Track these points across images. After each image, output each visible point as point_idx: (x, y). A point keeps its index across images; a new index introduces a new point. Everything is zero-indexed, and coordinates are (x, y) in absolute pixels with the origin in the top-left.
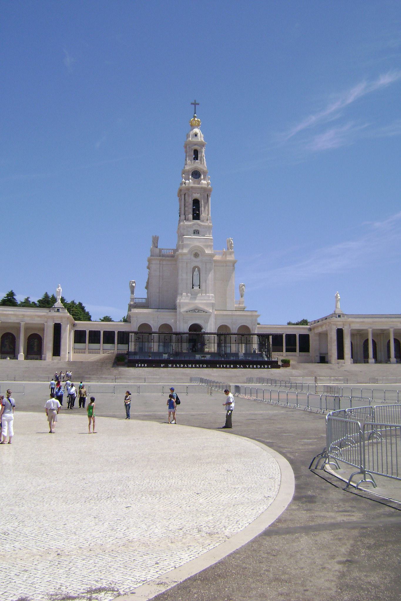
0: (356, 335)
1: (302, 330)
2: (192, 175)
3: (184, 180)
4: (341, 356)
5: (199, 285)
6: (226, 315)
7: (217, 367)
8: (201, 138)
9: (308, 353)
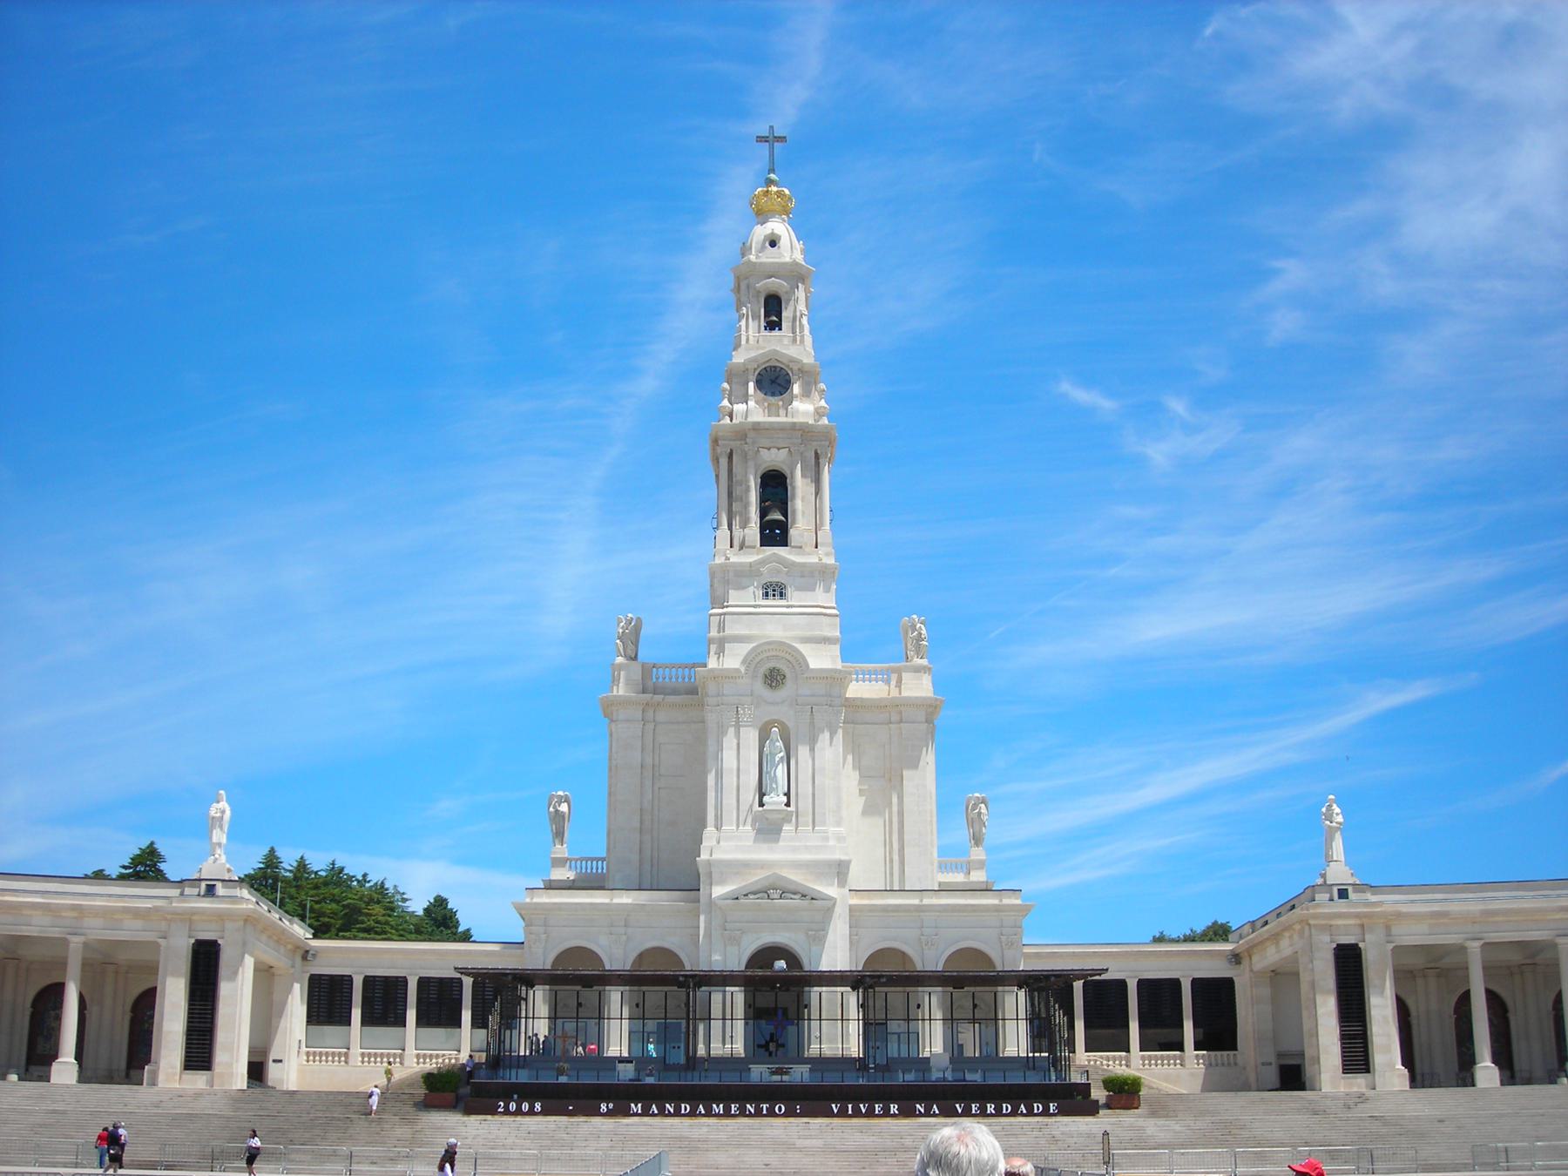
0: (1425, 976)
1: (1209, 962)
2: (760, 384)
3: (726, 403)
4: (1357, 1057)
5: (788, 795)
6: (897, 908)
7: (830, 1114)
8: (791, 250)
9: (1231, 1053)
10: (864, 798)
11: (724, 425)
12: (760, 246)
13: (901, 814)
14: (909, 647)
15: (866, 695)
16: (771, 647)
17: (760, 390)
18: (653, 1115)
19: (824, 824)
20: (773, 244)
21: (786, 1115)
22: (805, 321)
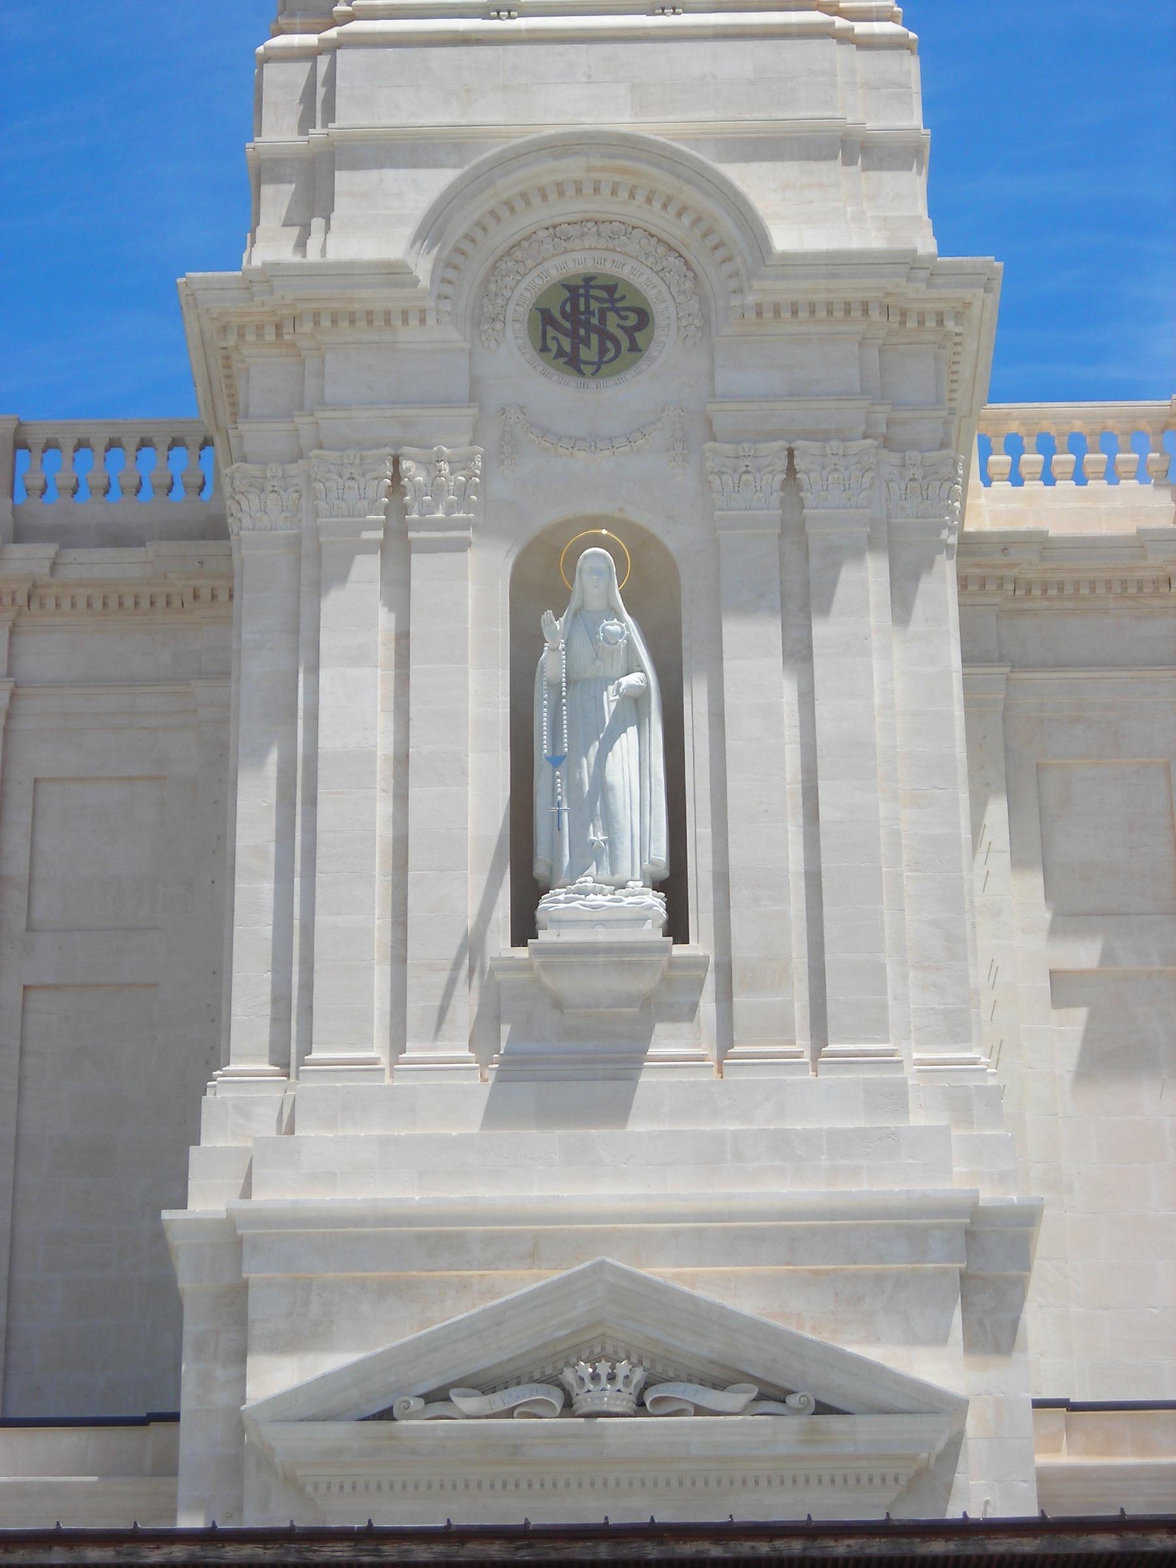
10: (1080, 1014)
15: (1057, 528)
16: (572, 168)
19: (880, 1029)
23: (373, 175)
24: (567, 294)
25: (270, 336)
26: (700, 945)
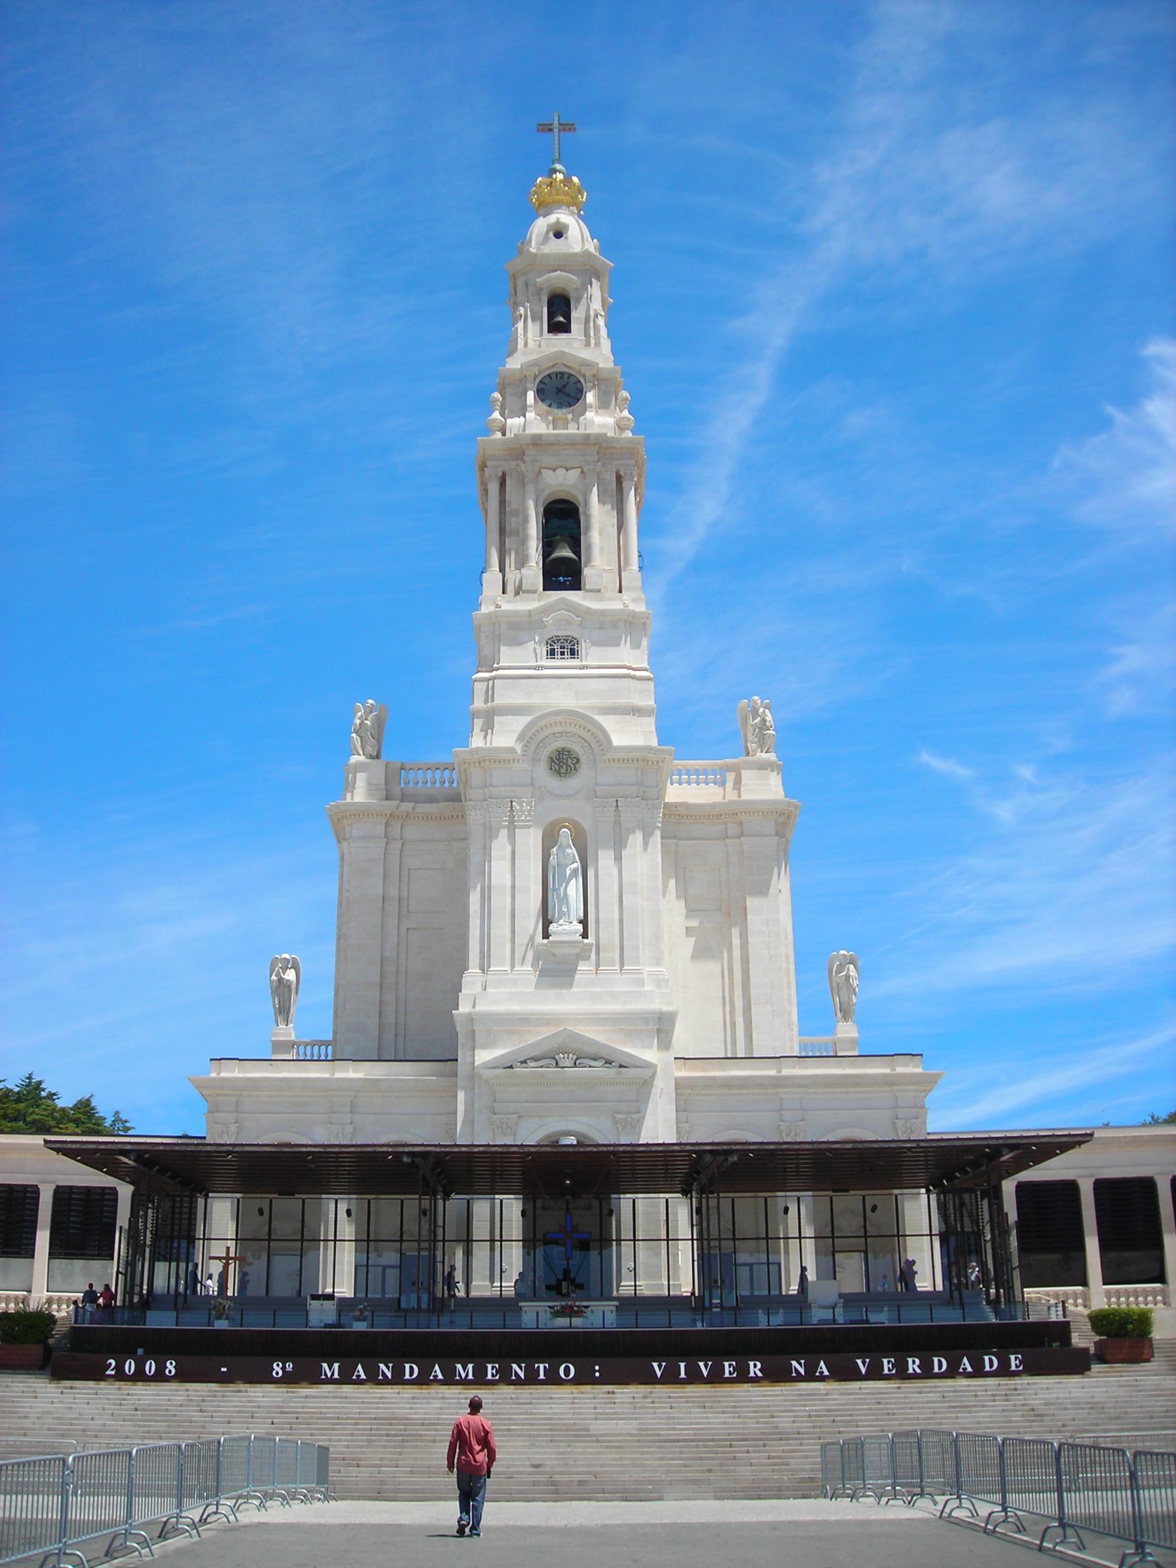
2: (541, 393)
3: (496, 415)
5: (584, 922)
7: (650, 1379)
10: (694, 939)
11: (494, 440)
12: (542, 238)
13: (745, 960)
14: (750, 737)
16: (559, 718)
17: (543, 400)
18: (359, 1382)
19: (637, 963)
20: (558, 235)
21: (577, 1381)
22: (601, 322)
23: (505, 717)
24: (557, 753)
25: (477, 765)
26: (591, 940)
